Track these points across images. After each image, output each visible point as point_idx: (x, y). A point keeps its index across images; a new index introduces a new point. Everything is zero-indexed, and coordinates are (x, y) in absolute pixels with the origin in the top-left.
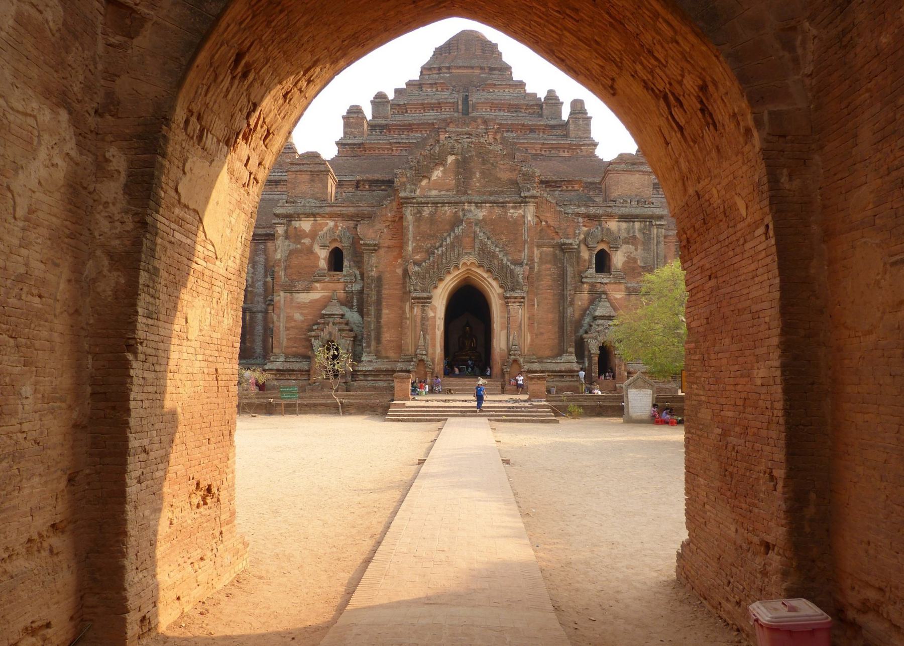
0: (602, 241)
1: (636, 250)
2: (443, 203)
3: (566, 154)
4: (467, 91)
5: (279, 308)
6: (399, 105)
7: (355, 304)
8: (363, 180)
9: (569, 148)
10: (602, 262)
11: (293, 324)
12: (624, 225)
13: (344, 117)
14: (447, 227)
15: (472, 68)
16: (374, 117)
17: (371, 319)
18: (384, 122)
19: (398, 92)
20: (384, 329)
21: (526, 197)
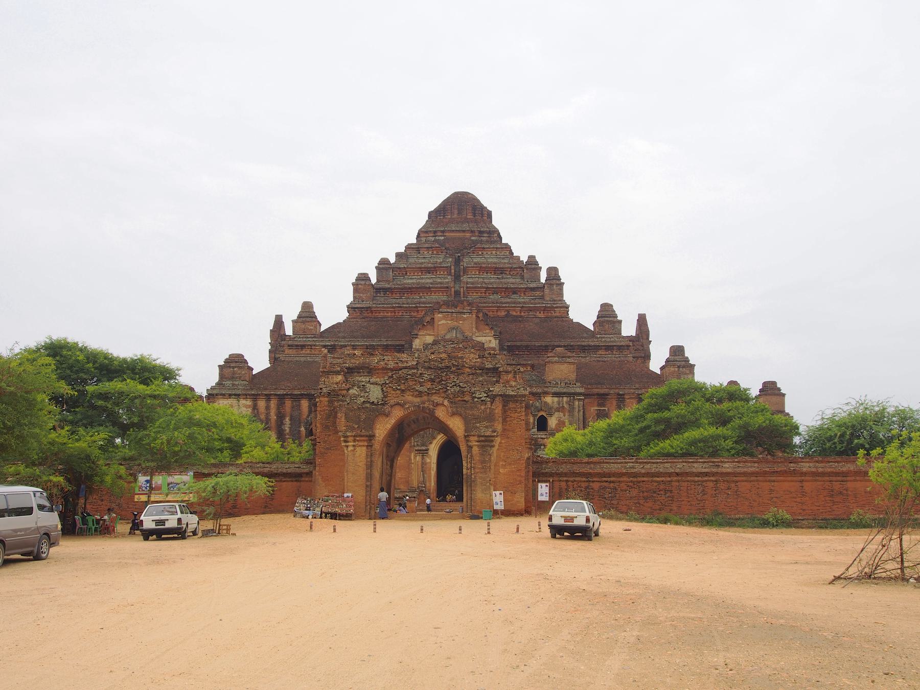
3: (542, 315)
9: (545, 309)
12: (556, 399)
13: (353, 284)
15: (464, 231)
16: (378, 281)
18: (387, 286)
19: (398, 255)
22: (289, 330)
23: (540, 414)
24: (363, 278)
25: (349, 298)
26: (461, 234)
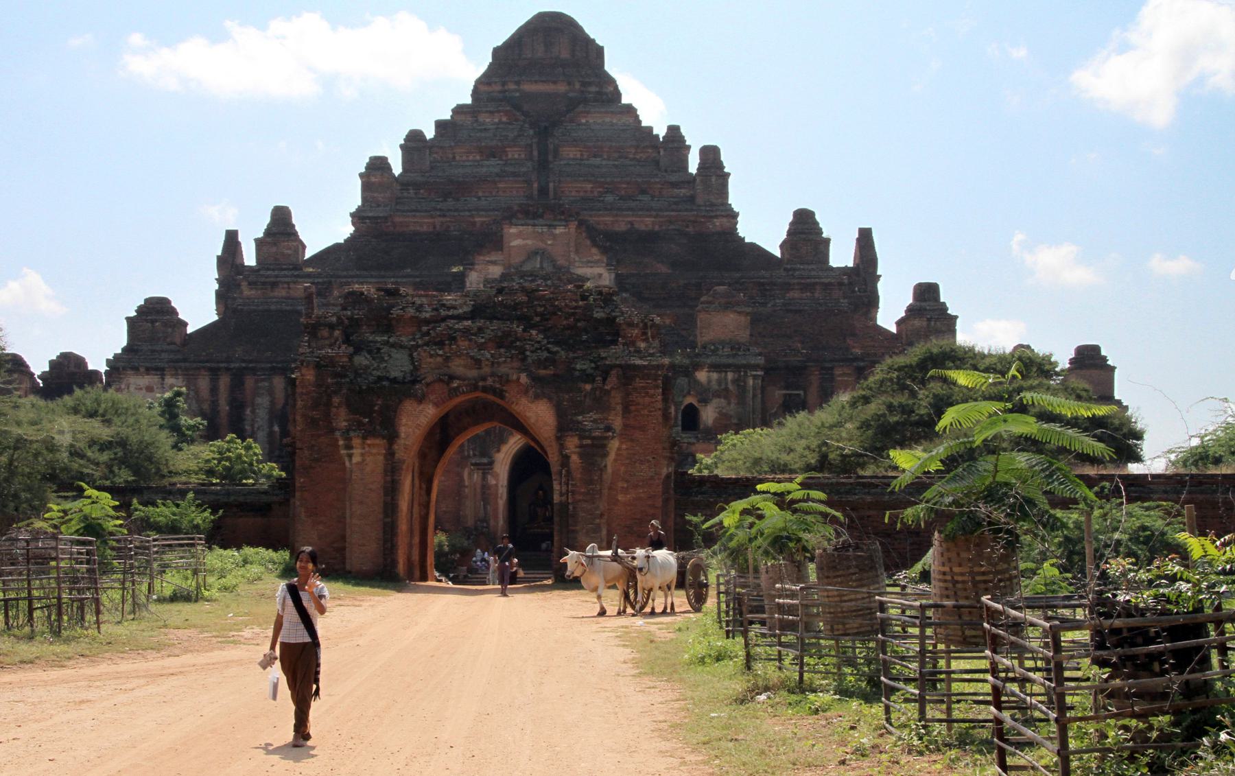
1: (729, 404)
12: (715, 376)
13: (361, 175)
19: (440, 125)
22: (250, 258)
23: (689, 400)
24: (378, 165)
25: (356, 201)
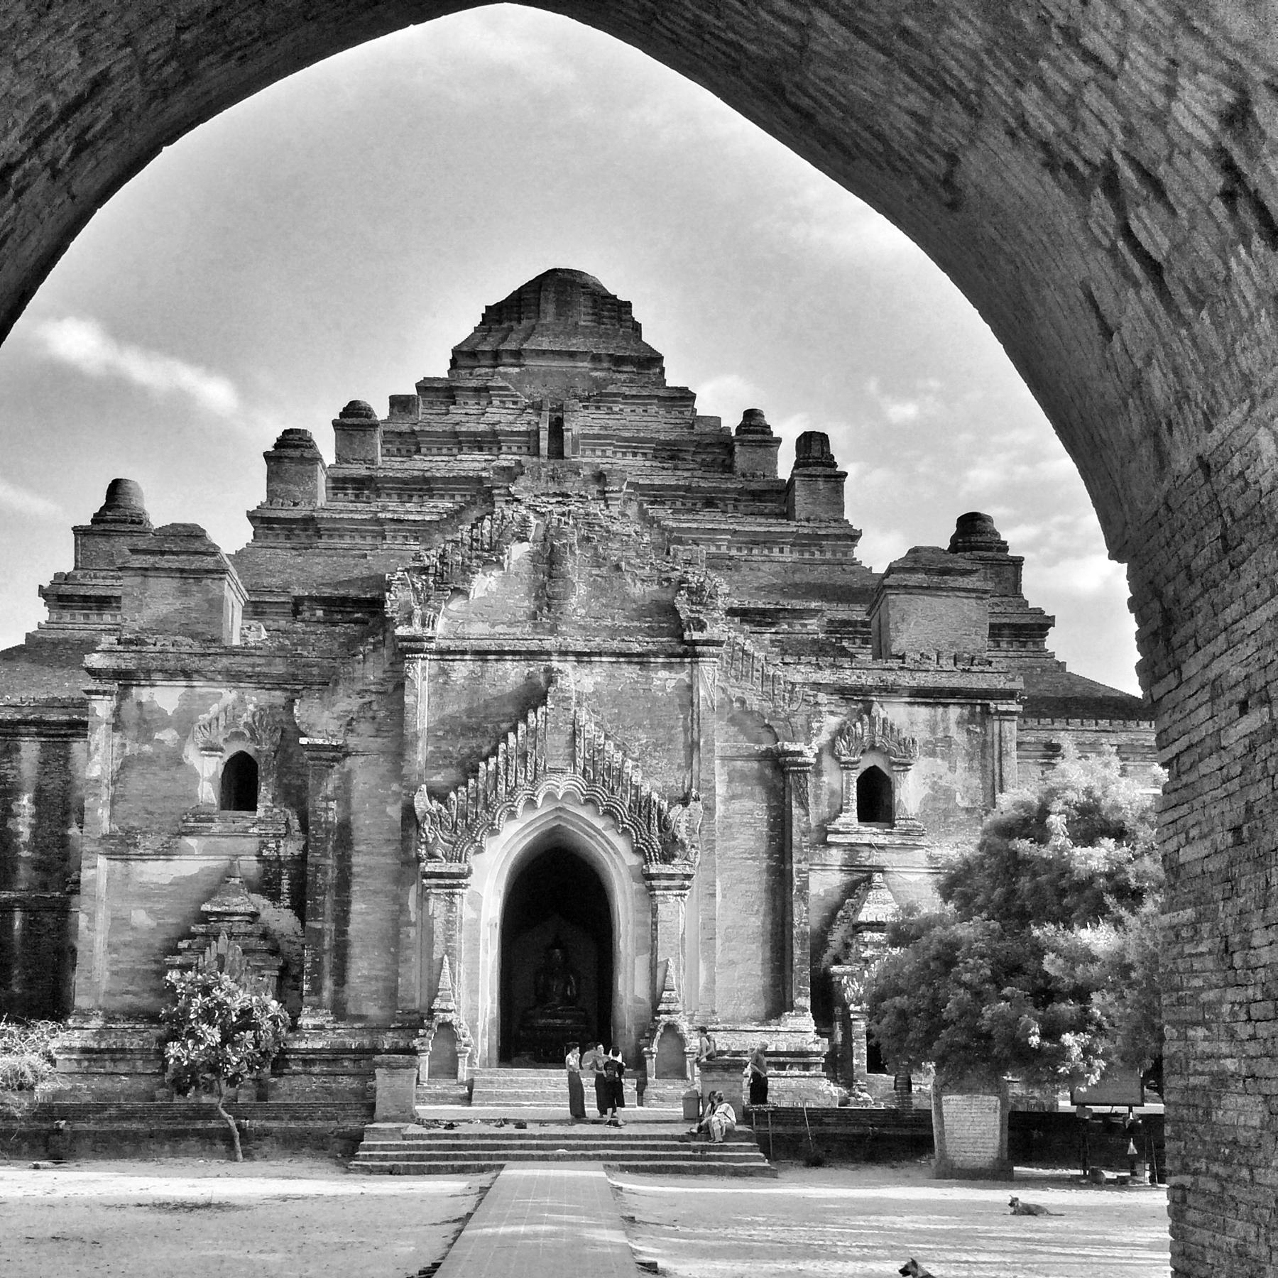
0: (873, 748)
1: (952, 769)
2: (501, 654)
4: (560, 409)
5: (93, 897)
6: (400, 434)
7: (285, 887)
8: (311, 598)
10: (875, 799)
11: (128, 937)
12: (923, 713)
14: (510, 709)
15: (572, 355)
17: (326, 925)
20: (355, 950)
21: (695, 643)
23: (867, 762)
26: (566, 364)
